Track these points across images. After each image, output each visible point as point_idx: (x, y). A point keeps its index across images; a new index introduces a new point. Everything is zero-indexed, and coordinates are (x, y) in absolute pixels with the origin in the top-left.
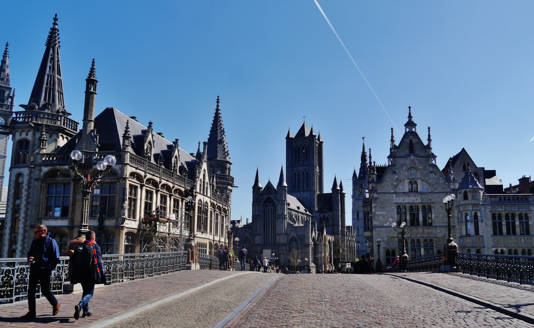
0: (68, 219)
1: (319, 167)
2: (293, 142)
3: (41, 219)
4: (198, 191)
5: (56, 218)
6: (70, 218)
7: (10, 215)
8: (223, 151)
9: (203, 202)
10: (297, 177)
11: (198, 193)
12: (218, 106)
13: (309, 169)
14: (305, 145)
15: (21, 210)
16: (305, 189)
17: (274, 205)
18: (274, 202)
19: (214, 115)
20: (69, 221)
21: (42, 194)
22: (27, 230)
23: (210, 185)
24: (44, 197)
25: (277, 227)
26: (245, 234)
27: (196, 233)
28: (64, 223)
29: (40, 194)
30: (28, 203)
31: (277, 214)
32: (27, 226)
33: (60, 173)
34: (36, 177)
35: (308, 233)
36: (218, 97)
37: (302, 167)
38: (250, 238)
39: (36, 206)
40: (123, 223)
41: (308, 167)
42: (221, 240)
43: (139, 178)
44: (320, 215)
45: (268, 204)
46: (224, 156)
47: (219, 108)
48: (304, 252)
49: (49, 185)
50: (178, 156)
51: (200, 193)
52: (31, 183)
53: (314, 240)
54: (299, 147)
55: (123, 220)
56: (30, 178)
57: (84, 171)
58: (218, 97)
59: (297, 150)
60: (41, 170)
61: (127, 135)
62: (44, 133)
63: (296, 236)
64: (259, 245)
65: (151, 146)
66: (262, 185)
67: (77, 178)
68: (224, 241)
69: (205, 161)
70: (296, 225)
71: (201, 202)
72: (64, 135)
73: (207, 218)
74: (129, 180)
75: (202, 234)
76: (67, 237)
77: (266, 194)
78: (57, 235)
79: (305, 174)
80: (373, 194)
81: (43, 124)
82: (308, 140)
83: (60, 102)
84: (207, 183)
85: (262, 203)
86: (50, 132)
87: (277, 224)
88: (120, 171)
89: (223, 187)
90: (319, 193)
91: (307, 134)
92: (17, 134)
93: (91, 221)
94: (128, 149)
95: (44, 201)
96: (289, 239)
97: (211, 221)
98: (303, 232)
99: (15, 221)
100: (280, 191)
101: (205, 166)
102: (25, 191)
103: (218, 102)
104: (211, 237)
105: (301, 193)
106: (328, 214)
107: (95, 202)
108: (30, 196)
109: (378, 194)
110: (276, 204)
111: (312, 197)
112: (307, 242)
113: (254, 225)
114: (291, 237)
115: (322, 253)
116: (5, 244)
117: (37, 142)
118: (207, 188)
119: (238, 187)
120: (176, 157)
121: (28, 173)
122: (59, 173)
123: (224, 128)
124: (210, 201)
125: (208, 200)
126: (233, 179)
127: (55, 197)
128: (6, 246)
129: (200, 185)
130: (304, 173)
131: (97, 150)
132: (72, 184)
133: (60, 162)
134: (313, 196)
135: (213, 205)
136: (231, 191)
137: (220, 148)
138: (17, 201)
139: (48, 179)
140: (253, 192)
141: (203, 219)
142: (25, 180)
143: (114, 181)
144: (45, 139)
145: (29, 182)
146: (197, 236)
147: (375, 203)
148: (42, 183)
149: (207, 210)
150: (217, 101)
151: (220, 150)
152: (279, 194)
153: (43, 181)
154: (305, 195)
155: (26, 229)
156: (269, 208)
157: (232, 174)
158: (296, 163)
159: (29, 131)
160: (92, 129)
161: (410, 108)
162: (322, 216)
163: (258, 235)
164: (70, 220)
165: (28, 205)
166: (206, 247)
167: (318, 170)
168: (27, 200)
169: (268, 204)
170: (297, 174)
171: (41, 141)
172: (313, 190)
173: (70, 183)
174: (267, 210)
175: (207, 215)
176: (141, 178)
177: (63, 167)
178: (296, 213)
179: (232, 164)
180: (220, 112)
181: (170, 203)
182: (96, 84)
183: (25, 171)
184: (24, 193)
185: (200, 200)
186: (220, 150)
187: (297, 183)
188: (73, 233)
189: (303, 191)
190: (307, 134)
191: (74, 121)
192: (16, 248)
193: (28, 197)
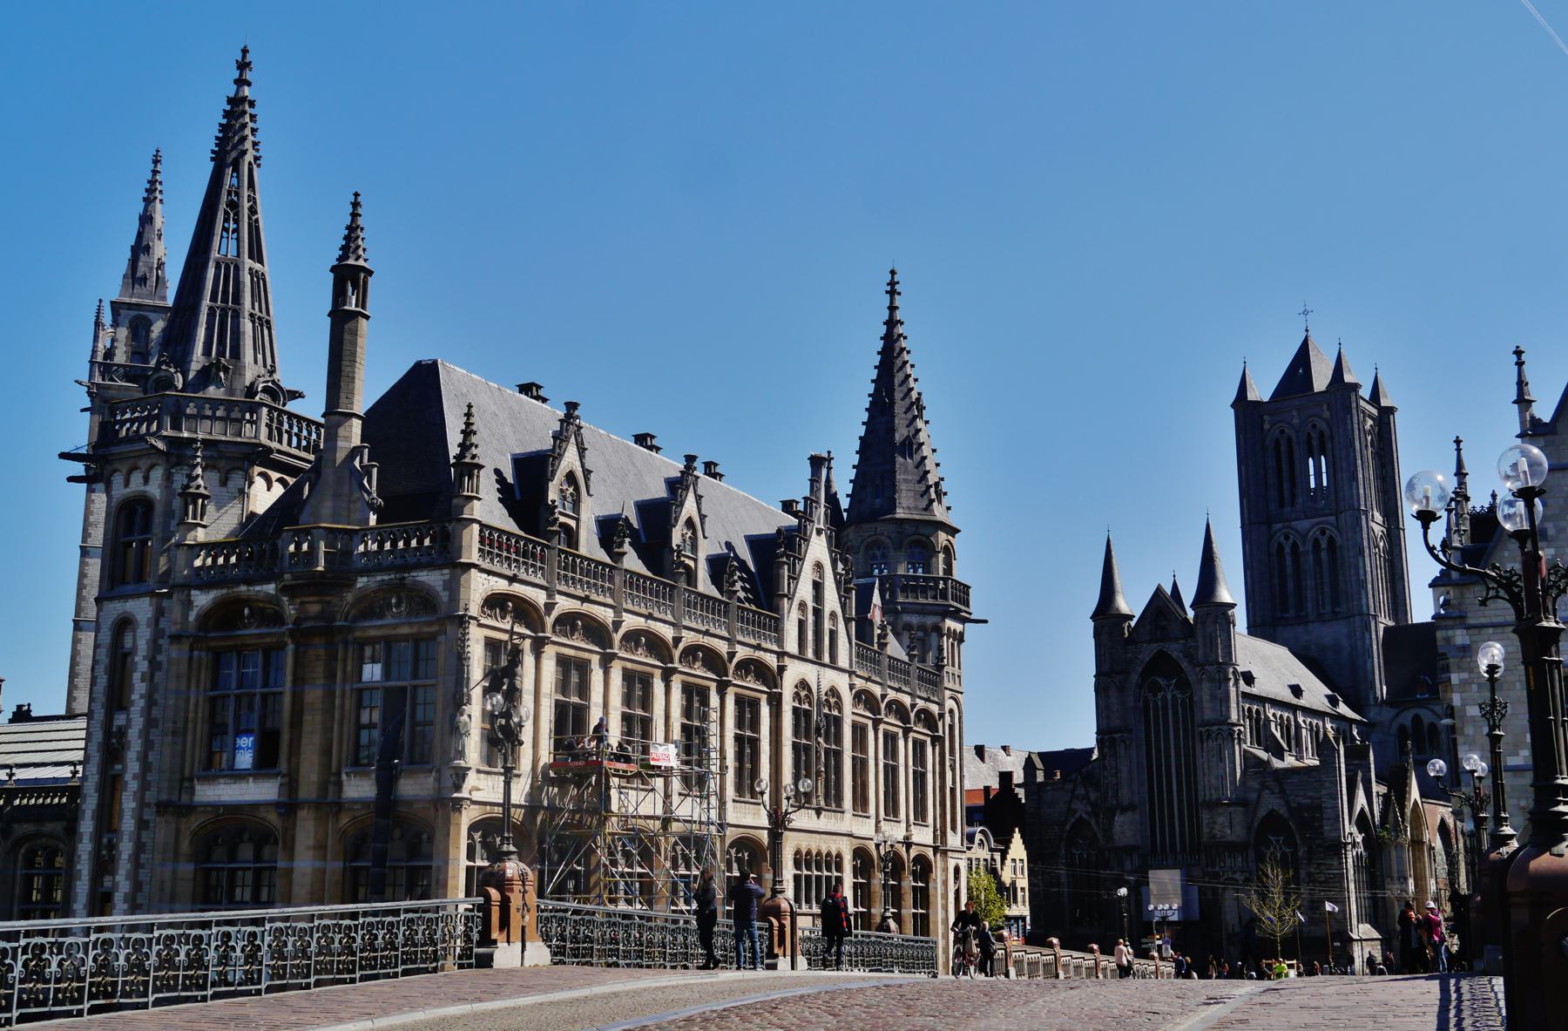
0: (276, 775)
1: (1385, 515)
2: (1263, 422)
3: (191, 779)
4: (791, 645)
5: (239, 776)
6: (284, 771)
8: (919, 482)
10: (1289, 561)
11: (792, 656)
12: (892, 308)
13: (1337, 527)
14: (1314, 426)
15: (129, 749)
16: (1328, 608)
17: (1184, 685)
18: (1182, 670)
19: (880, 345)
20: (281, 785)
21: (193, 688)
22: (147, 822)
23: (847, 621)
24: (201, 699)
25: (1200, 773)
26: (1074, 806)
28: (263, 791)
29: (189, 688)
30: (150, 723)
31: (1198, 719)
32: (148, 805)
33: (251, 610)
34: (174, 629)
35: (1334, 796)
36: (893, 273)
37: (1307, 517)
38: (1093, 822)
39: (174, 733)
40: (458, 788)
41: (1332, 519)
42: (915, 839)
43: (524, 611)
44: (1397, 715)
45: (1160, 680)
46: (924, 503)
47: (899, 315)
48: (1322, 879)
49: (218, 657)
50: (697, 520)
51: (801, 657)
52: (160, 653)
53: (1362, 822)
54: (1289, 440)
55: (457, 774)
56: (157, 634)
57: (328, 598)
58: (893, 273)
59: (1283, 448)
60: (188, 604)
61: (467, 460)
62: (199, 471)
63: (1283, 811)
64: (1130, 850)
65: (577, 489)
66: (1132, 603)
67: (304, 625)
68: (931, 843)
69: (819, 532)
70: (1290, 761)
71: (810, 690)
72: (270, 473)
73: (838, 755)
74: (481, 625)
75: (818, 814)
76: (276, 842)
77: (1149, 642)
78: (246, 836)
79: (1324, 545)
80: (1450, 633)
81: (195, 440)
82: (1325, 407)
83: (260, 357)
84: (833, 615)
85: (1135, 678)
86: (222, 464)
87: (1199, 762)
88: (447, 593)
89: (922, 627)
90: (1391, 623)
91: (1321, 380)
92: (118, 480)
93: (353, 783)
94: (472, 509)
95: (200, 715)
96: (1256, 824)
97: (860, 766)
98: (1309, 794)
99: (110, 785)
100: (1204, 623)
101: (818, 549)
102: (142, 681)
103: (892, 293)
104: (865, 828)
105: (1310, 626)
106: (1433, 712)
107: (368, 711)
108: (157, 697)
109: (1472, 631)
110: (1192, 679)
111: (1359, 643)
112: (1334, 834)
113: (1105, 768)
114: (1262, 812)
115: (1406, 879)
116: (80, 871)
117: (177, 503)
118: (833, 634)
119: (986, 622)
120: (690, 523)
121: (150, 615)
122: (246, 611)
123: (919, 394)
124: (852, 687)
125: (842, 682)
126: (963, 592)
127: (238, 697)
128: (83, 878)
129: (802, 625)
130: (1316, 543)
131: (373, 519)
132: (290, 647)
133: (251, 572)
134: (1363, 638)
135: (863, 698)
136: (960, 638)
137: (906, 472)
138: (116, 716)
139: (212, 635)
140: (1097, 635)
141: (818, 758)
142: (140, 640)
144: (202, 490)
145: (155, 646)
147: (1461, 669)
148: (191, 650)
149: (838, 722)
150: (889, 288)
151: (906, 481)
152: (1200, 639)
153: (196, 641)
154: (1327, 633)
155: (145, 817)
156: (1164, 699)
157: (959, 574)
158: (1282, 506)
159: (152, 467)
160: (353, 445)
162: (1407, 718)
163: (1124, 810)
164: (286, 780)
165: (152, 730)
166: (839, 868)
167: (1378, 530)
168: (147, 712)
169: (1160, 680)
170: (1288, 550)
171: (189, 500)
172: (1361, 614)
173: (282, 646)
174: (1155, 703)
175: (838, 739)
176: (535, 615)
177: (258, 588)
178: (1286, 715)
179: (958, 531)
180: (900, 330)
181: (668, 705)
182: (365, 283)
183: (142, 609)
184: (139, 687)
185: (803, 684)
186: (906, 481)
187: (1290, 585)
188: (294, 829)
189: (1320, 618)
190: (1321, 380)
191: (305, 419)
192: (115, 886)
193: (150, 701)
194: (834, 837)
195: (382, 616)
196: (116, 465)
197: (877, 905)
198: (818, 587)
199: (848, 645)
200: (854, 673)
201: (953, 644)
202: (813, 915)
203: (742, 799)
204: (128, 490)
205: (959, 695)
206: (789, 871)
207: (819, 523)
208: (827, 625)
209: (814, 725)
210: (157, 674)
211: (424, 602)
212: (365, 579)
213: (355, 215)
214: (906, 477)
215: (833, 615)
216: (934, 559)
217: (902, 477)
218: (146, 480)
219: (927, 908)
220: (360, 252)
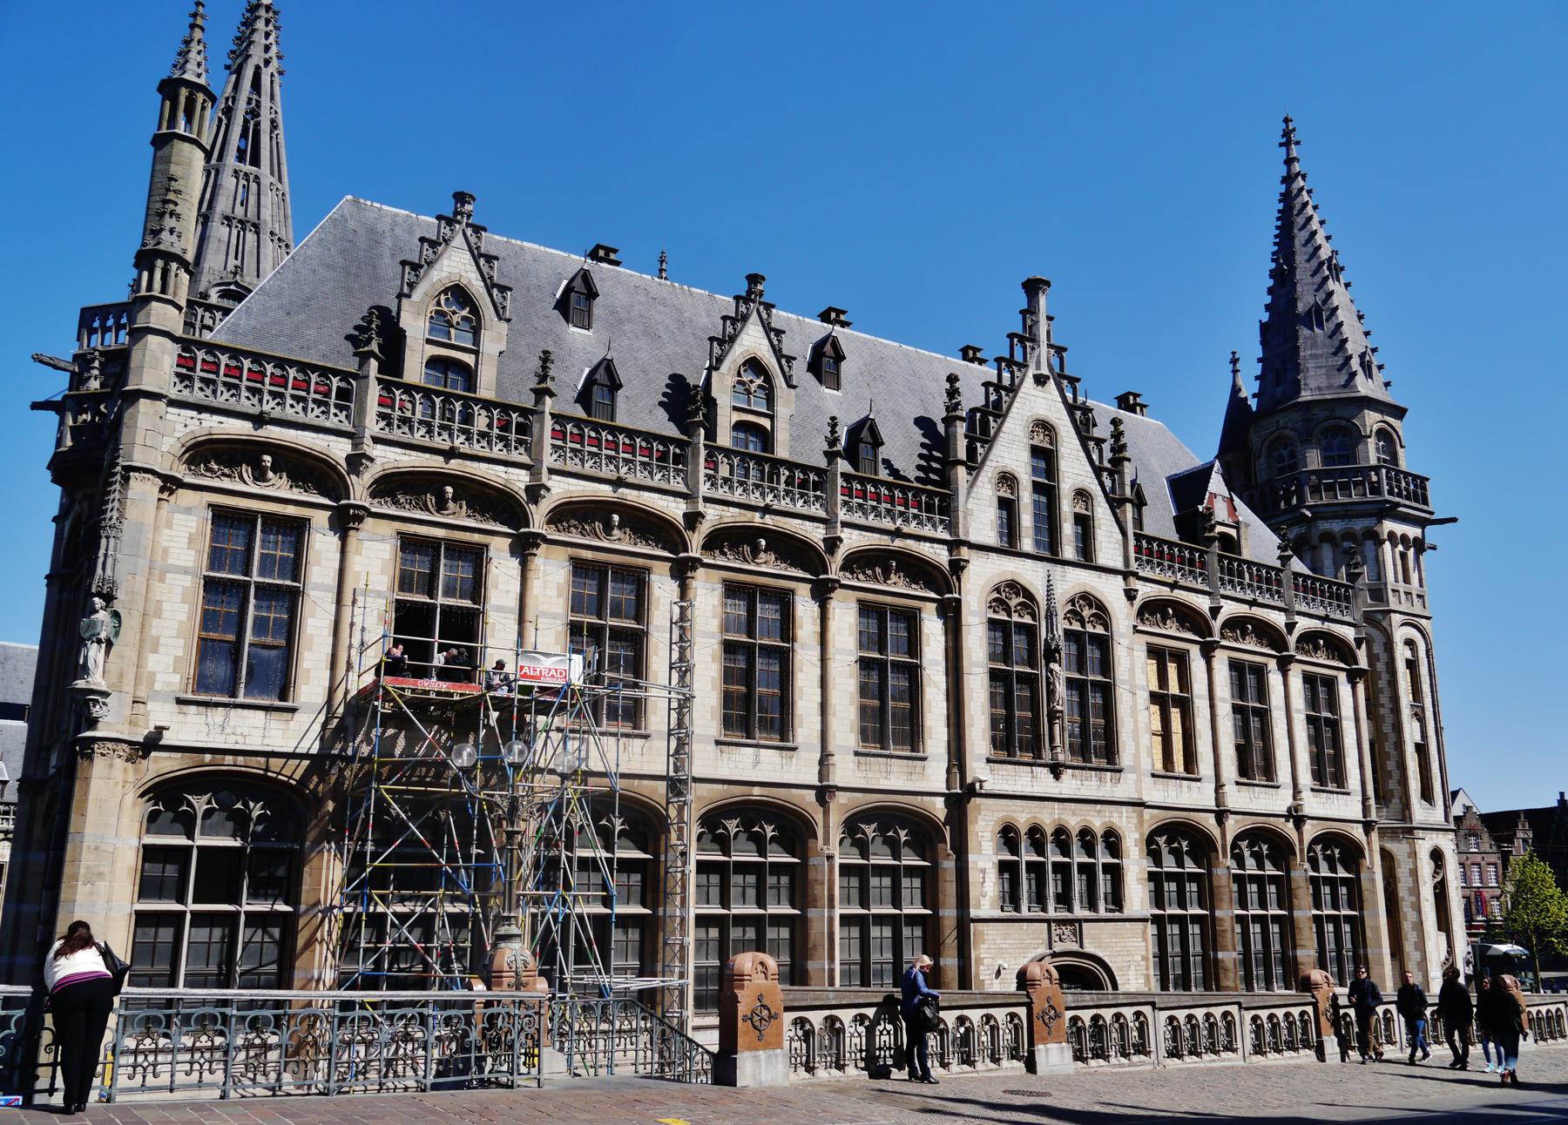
8: (1335, 354)
9: (1041, 596)
27: (977, 768)
42: (1308, 810)
46: (1342, 378)
68: (1360, 817)
71: (1029, 595)
75: (1057, 776)
89: (1349, 535)
94: (148, 315)
118: (1084, 523)
119: (1454, 520)
124: (1130, 595)
126: (1418, 487)
137: (1314, 345)
146: (988, 787)
151: (1314, 356)
186: (1314, 356)
194: (1098, 807)
197: (1225, 905)
198: (1045, 457)
199: (1120, 536)
200: (1135, 575)
201: (1403, 556)
202: (1048, 921)
203: (914, 754)
205: (1423, 622)
206: (984, 856)
207: (1038, 366)
208: (1067, 508)
209: (1041, 646)
214: (1314, 352)
215: (1082, 494)
216: (1361, 447)
217: (1309, 352)
219: (1361, 909)
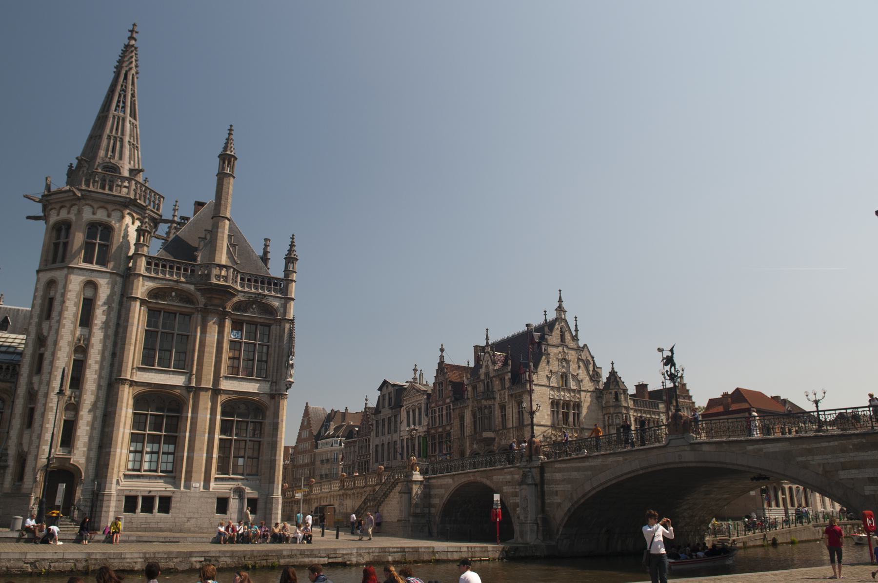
7: (65, 355)
32: (103, 378)
33: (176, 293)
57: (224, 298)
61: (292, 256)
67: (209, 307)
88: (282, 309)
122: (174, 294)
143: (268, 322)
144: (148, 229)
148: (141, 306)
153: (143, 302)
155: (101, 384)
161: (560, 291)
171: (142, 233)
173: (190, 315)
195: (246, 312)
196: (88, 202)
204: (95, 217)
210: (112, 313)
211: (269, 310)
212: (243, 294)
213: (230, 134)
218: (109, 216)
220: (232, 149)
